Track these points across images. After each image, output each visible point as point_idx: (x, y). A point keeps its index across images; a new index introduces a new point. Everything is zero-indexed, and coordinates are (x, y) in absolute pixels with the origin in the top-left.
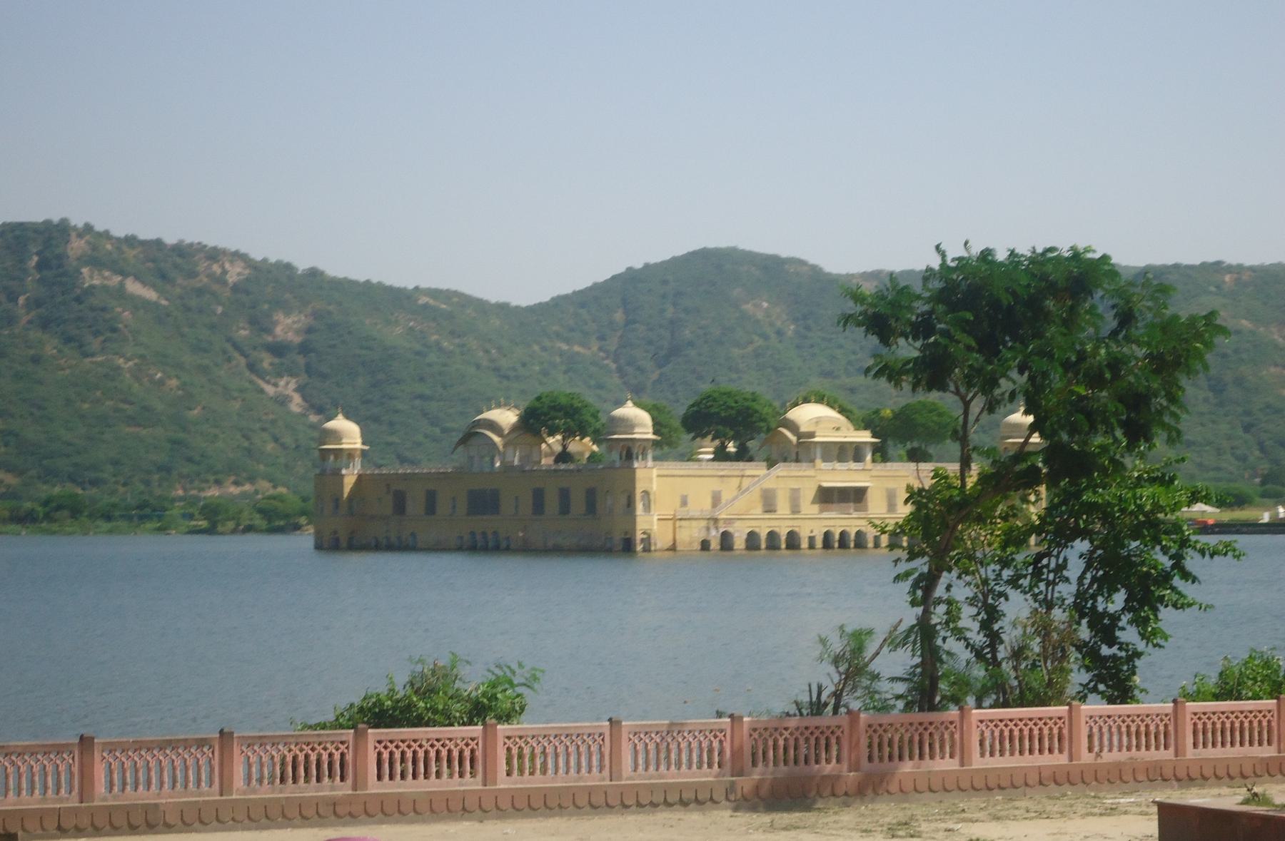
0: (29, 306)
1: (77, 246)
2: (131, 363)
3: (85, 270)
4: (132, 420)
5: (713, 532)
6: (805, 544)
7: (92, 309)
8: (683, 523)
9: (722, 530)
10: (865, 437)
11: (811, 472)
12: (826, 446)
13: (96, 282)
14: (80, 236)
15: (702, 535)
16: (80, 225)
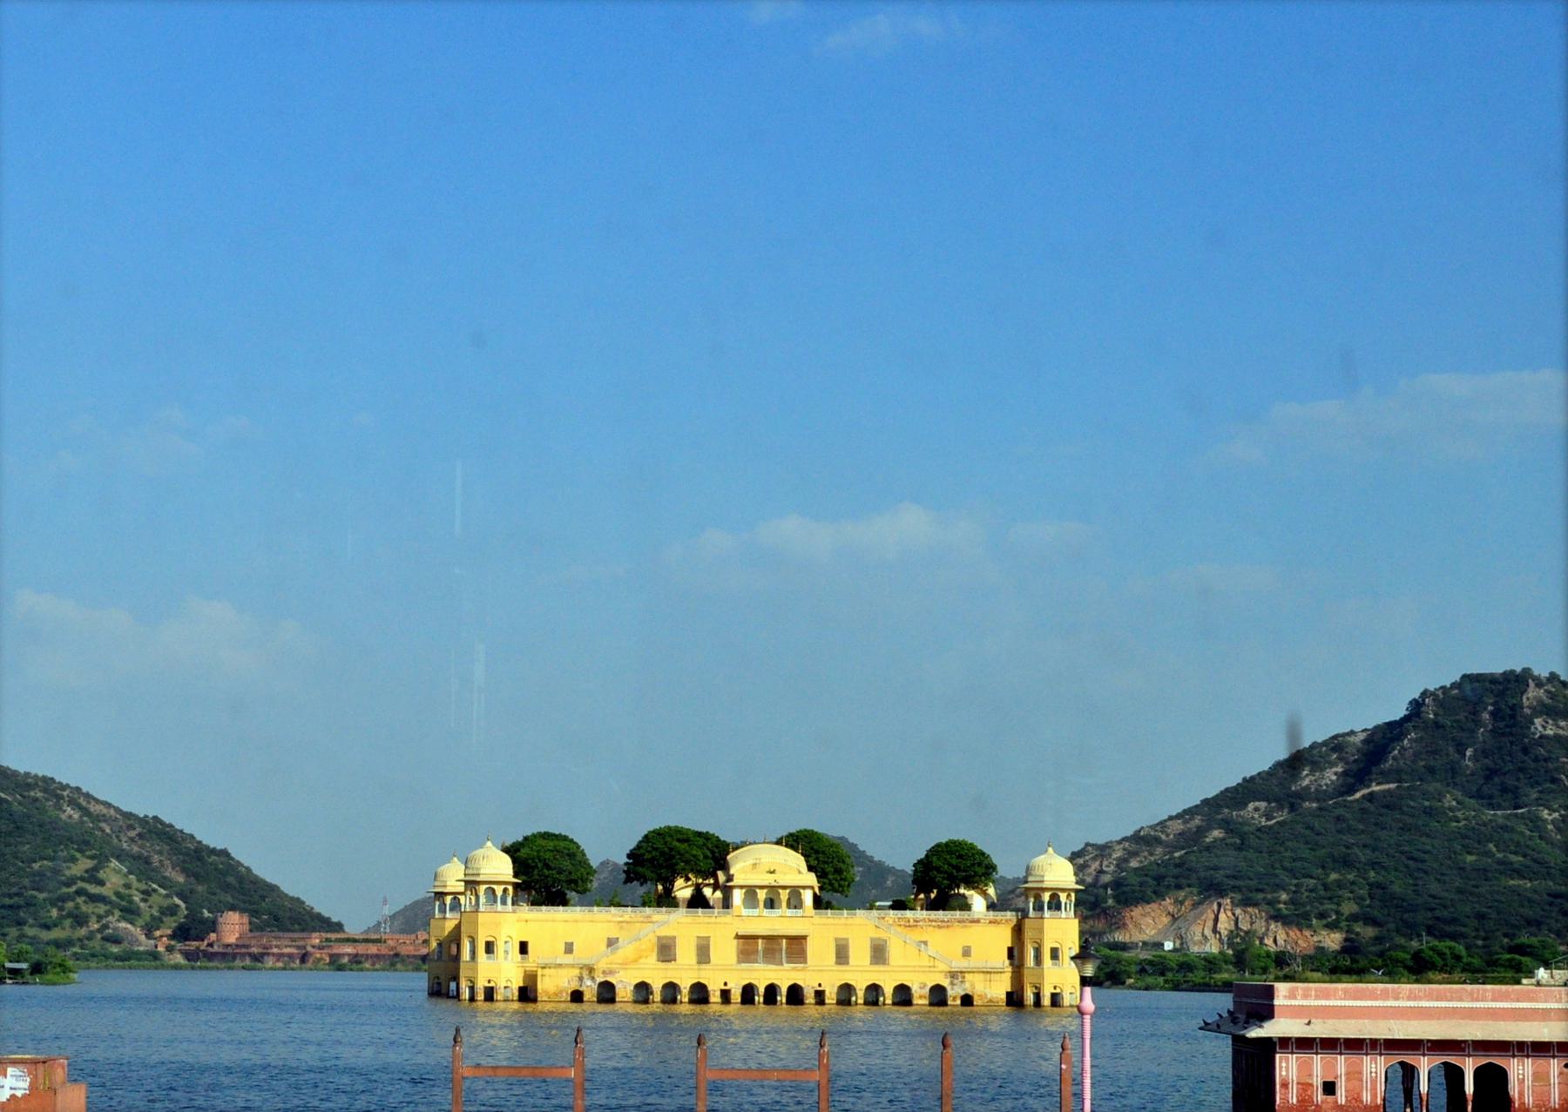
0: (1475, 758)
1: (1533, 694)
2: (1556, 815)
3: (1538, 721)
4: (1518, 873)
5: (589, 983)
6: (715, 998)
7: (1536, 760)
8: (547, 971)
9: (600, 979)
10: (811, 879)
11: (727, 919)
12: (751, 891)
13: (1550, 732)
14: (1539, 684)
15: (574, 986)
16: (1545, 674)
